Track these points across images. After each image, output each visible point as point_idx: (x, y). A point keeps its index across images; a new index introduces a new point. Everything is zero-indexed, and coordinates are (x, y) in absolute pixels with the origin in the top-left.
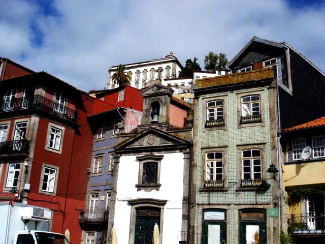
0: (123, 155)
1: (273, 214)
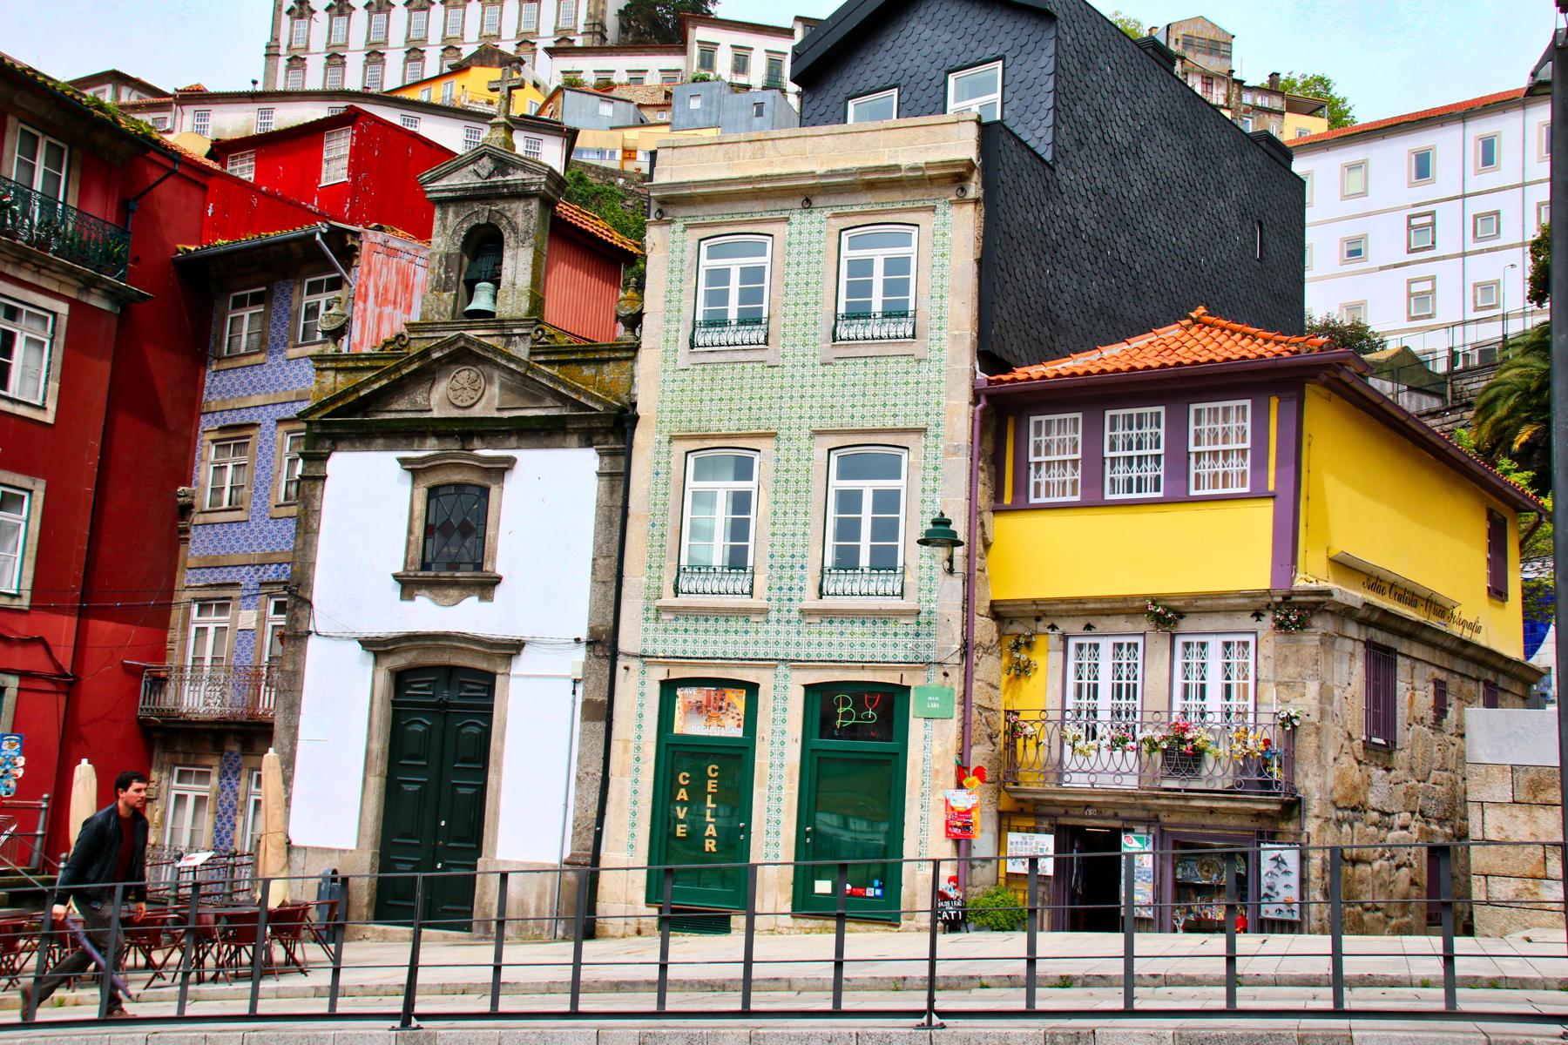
0: (340, 446)
1: (934, 705)
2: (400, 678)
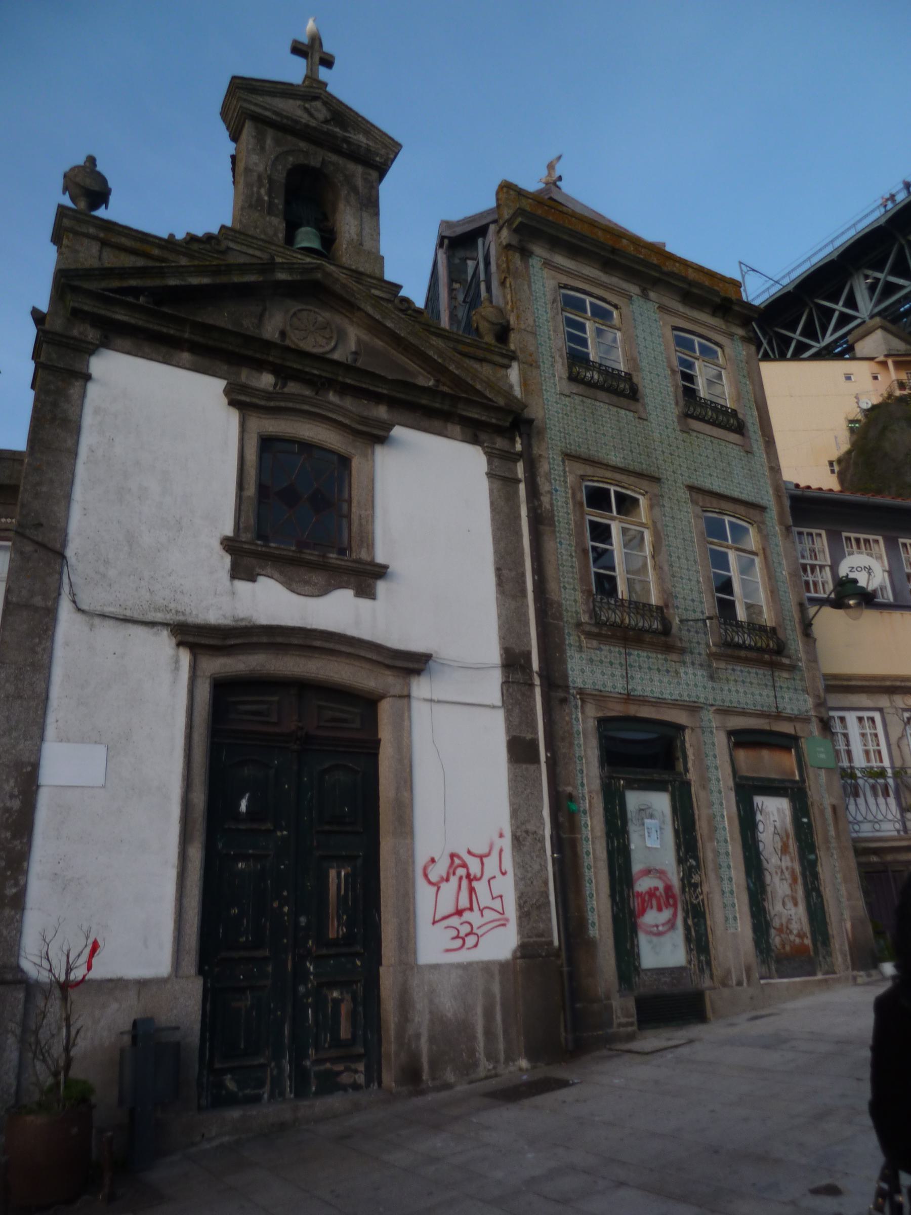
0: (119, 342)
2: (224, 690)
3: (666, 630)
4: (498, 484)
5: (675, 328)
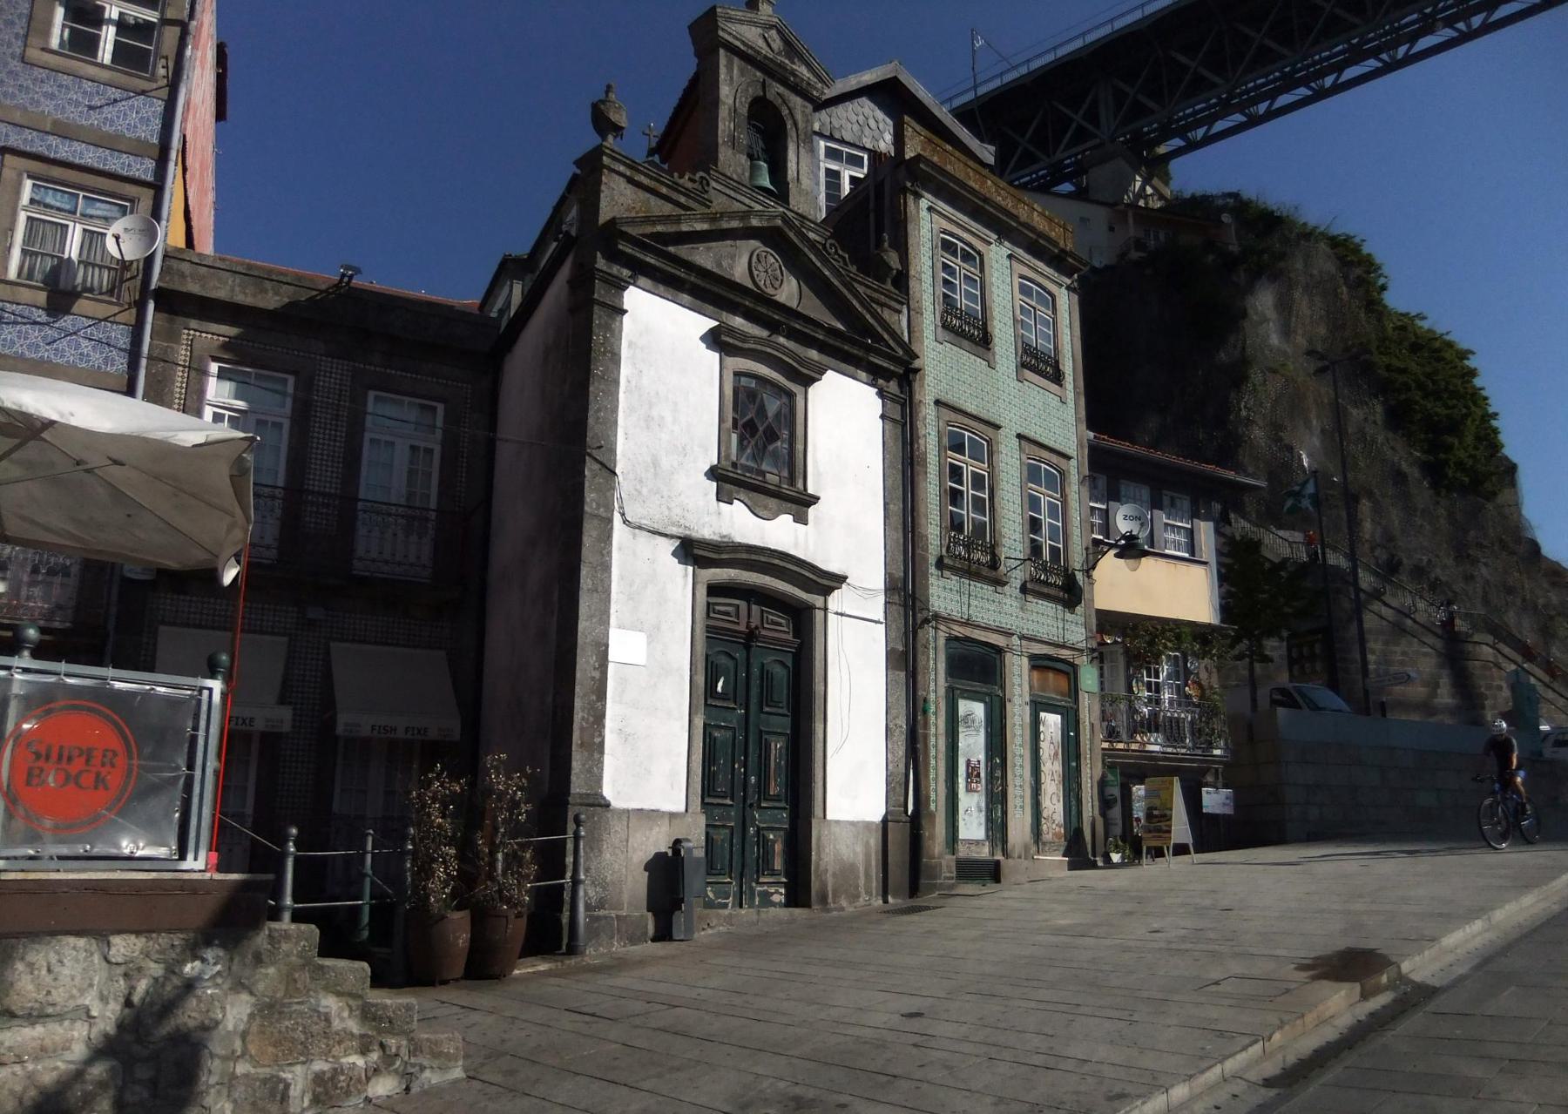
0: (642, 281)
3: (994, 564)
4: (889, 426)
5: (1022, 277)
